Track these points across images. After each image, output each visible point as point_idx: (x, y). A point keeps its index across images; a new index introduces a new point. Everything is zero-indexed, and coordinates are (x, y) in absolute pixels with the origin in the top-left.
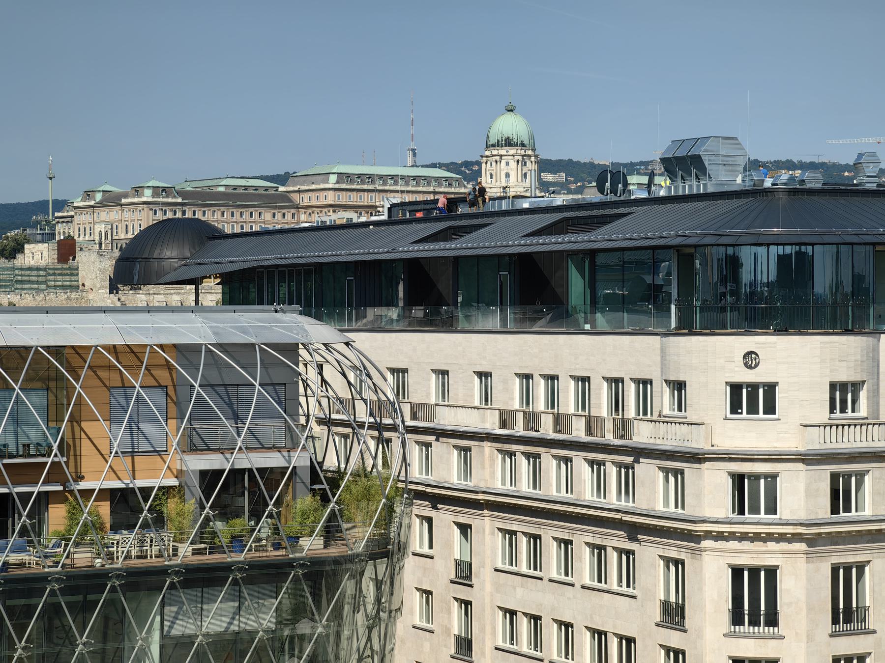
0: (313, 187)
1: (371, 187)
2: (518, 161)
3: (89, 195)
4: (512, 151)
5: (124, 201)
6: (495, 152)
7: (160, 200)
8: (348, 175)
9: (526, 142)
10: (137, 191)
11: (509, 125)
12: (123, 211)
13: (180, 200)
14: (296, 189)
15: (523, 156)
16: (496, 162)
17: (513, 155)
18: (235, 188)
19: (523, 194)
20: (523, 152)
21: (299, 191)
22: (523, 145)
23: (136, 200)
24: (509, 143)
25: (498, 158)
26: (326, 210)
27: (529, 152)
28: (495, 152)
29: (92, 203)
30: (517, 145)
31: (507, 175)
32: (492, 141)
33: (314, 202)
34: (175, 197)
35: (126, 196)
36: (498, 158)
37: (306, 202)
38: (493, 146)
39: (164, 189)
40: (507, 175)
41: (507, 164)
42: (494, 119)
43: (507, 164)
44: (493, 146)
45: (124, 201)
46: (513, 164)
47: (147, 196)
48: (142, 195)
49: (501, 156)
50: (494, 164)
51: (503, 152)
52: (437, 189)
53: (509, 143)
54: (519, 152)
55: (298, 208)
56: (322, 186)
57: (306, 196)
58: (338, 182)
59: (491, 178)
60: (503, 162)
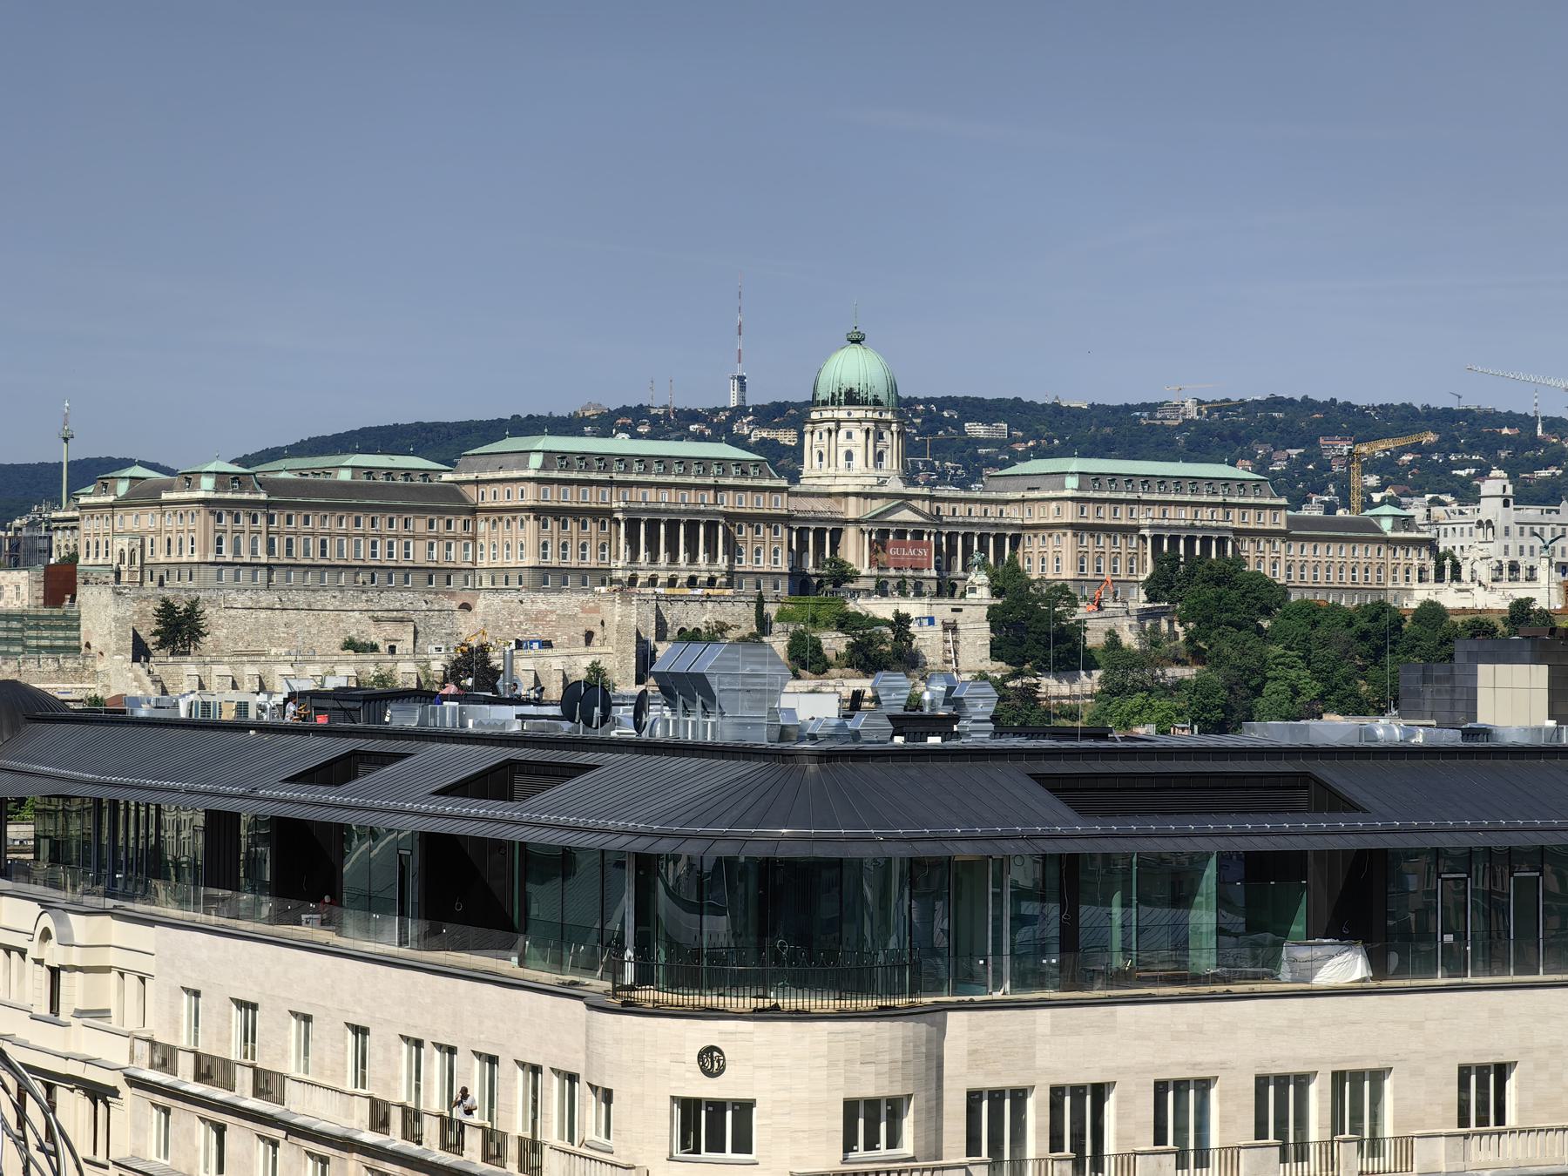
0: (501, 475)
2: (867, 432)
3: (106, 485)
4: (858, 414)
5: (165, 496)
7: (229, 496)
8: (564, 455)
9: (882, 398)
10: (188, 480)
12: (163, 514)
13: (263, 497)
14: (472, 477)
15: (876, 422)
16: (830, 431)
17: (859, 421)
18: (370, 472)
19: (876, 490)
20: (876, 416)
21: (477, 482)
22: (877, 402)
23: (186, 495)
24: (852, 398)
25: (832, 425)
26: (522, 515)
28: (827, 415)
29: (111, 499)
30: (865, 403)
31: (849, 456)
32: (823, 394)
33: (502, 502)
34: (255, 492)
36: (832, 425)
37: (489, 502)
38: (825, 403)
39: (236, 477)
40: (849, 456)
41: (849, 435)
42: (826, 356)
43: (849, 435)
44: (825, 403)
45: (165, 496)
46: (859, 436)
48: (197, 487)
49: (838, 422)
50: (825, 435)
51: (842, 414)
52: (721, 481)
53: (852, 398)
54: (870, 415)
55: (474, 511)
56: (516, 474)
57: (489, 490)
58: (544, 467)
59: (821, 459)
60: (842, 433)
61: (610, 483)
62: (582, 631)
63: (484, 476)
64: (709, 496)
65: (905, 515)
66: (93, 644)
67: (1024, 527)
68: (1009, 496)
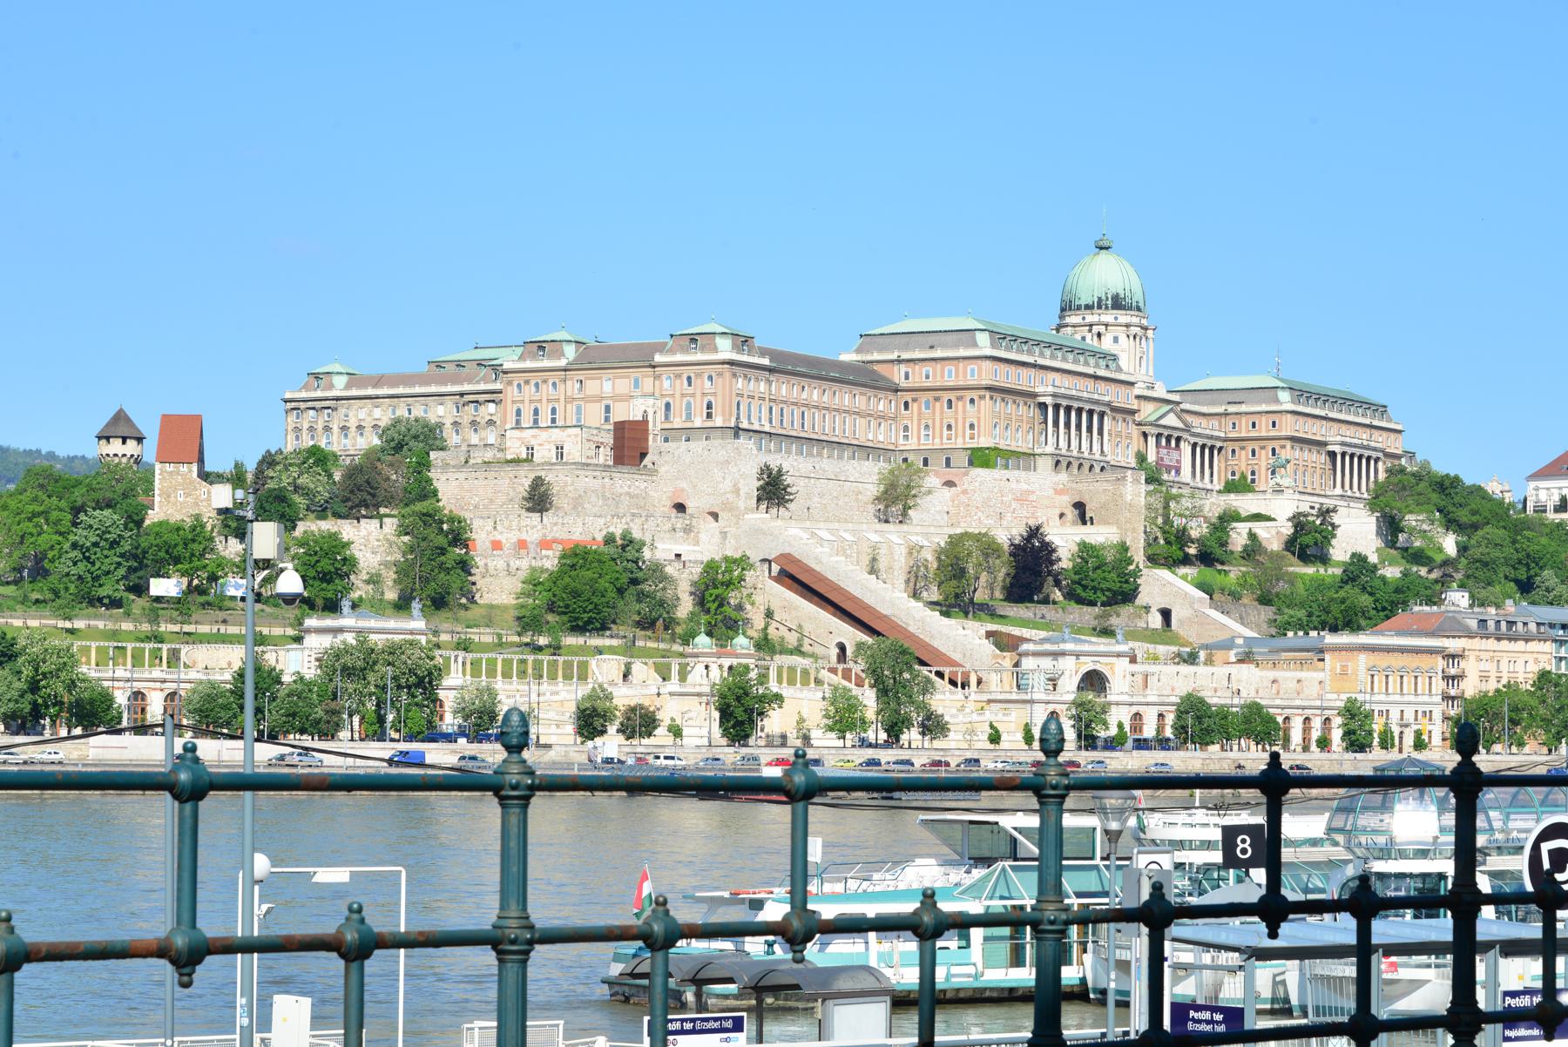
0: (938, 353)
1: (1030, 360)
3: (542, 348)
6: (1090, 319)
11: (1106, 274)
13: (766, 361)
14: (894, 356)
17: (1127, 326)
21: (899, 361)
22: (1139, 309)
24: (1118, 303)
26: (974, 394)
27: (1145, 322)
28: (1090, 319)
29: (562, 363)
35: (660, 348)
41: (1116, 340)
43: (1116, 340)
44: (1088, 307)
45: (658, 358)
47: (725, 349)
51: (1108, 317)
53: (1118, 303)
54: (1135, 320)
61: (1034, 366)
62: (1058, 512)
63: (905, 356)
64: (1090, 383)
65: (1171, 420)
66: (690, 505)
67: (1226, 440)
68: (1205, 409)
